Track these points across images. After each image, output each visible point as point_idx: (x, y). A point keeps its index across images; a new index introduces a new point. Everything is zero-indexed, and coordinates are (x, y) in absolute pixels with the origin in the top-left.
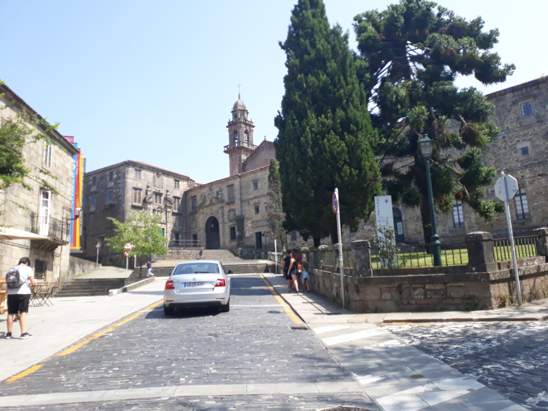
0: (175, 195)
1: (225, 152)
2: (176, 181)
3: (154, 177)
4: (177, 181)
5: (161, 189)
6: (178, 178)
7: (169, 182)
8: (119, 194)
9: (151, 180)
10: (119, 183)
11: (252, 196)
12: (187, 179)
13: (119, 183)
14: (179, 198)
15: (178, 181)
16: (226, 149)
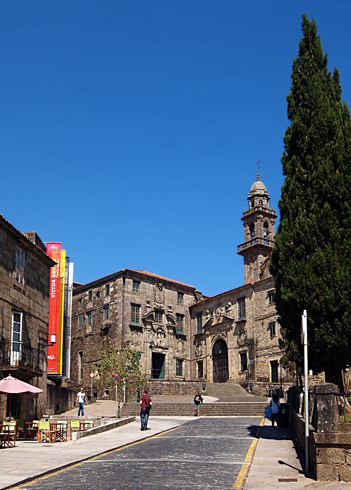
0: (178, 312)
1: (240, 253)
2: (179, 293)
3: (154, 290)
4: (181, 294)
5: (162, 305)
6: (182, 290)
7: (170, 294)
8: (116, 311)
9: (151, 293)
10: (116, 298)
11: (267, 313)
12: (191, 291)
13: (116, 298)
14: (183, 316)
15: (183, 294)
16: (241, 249)
